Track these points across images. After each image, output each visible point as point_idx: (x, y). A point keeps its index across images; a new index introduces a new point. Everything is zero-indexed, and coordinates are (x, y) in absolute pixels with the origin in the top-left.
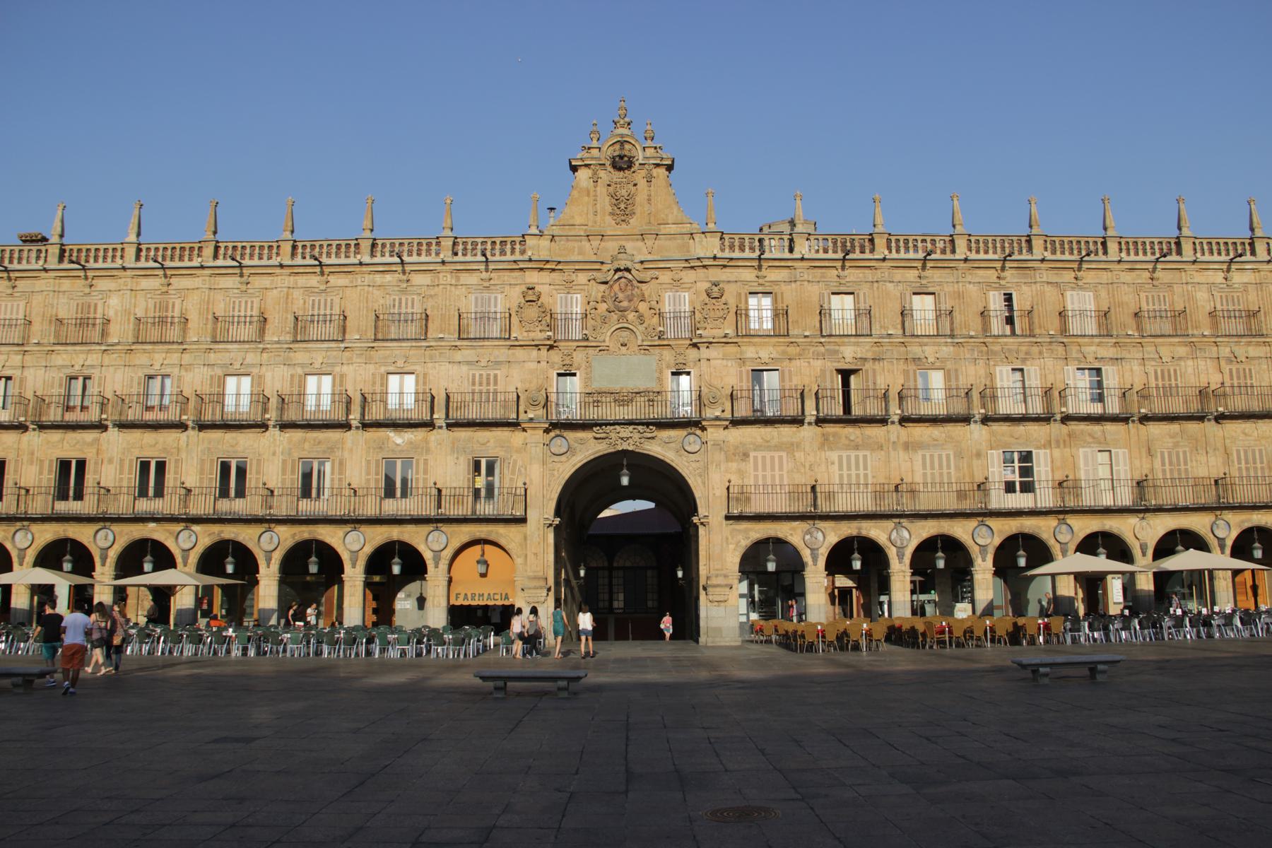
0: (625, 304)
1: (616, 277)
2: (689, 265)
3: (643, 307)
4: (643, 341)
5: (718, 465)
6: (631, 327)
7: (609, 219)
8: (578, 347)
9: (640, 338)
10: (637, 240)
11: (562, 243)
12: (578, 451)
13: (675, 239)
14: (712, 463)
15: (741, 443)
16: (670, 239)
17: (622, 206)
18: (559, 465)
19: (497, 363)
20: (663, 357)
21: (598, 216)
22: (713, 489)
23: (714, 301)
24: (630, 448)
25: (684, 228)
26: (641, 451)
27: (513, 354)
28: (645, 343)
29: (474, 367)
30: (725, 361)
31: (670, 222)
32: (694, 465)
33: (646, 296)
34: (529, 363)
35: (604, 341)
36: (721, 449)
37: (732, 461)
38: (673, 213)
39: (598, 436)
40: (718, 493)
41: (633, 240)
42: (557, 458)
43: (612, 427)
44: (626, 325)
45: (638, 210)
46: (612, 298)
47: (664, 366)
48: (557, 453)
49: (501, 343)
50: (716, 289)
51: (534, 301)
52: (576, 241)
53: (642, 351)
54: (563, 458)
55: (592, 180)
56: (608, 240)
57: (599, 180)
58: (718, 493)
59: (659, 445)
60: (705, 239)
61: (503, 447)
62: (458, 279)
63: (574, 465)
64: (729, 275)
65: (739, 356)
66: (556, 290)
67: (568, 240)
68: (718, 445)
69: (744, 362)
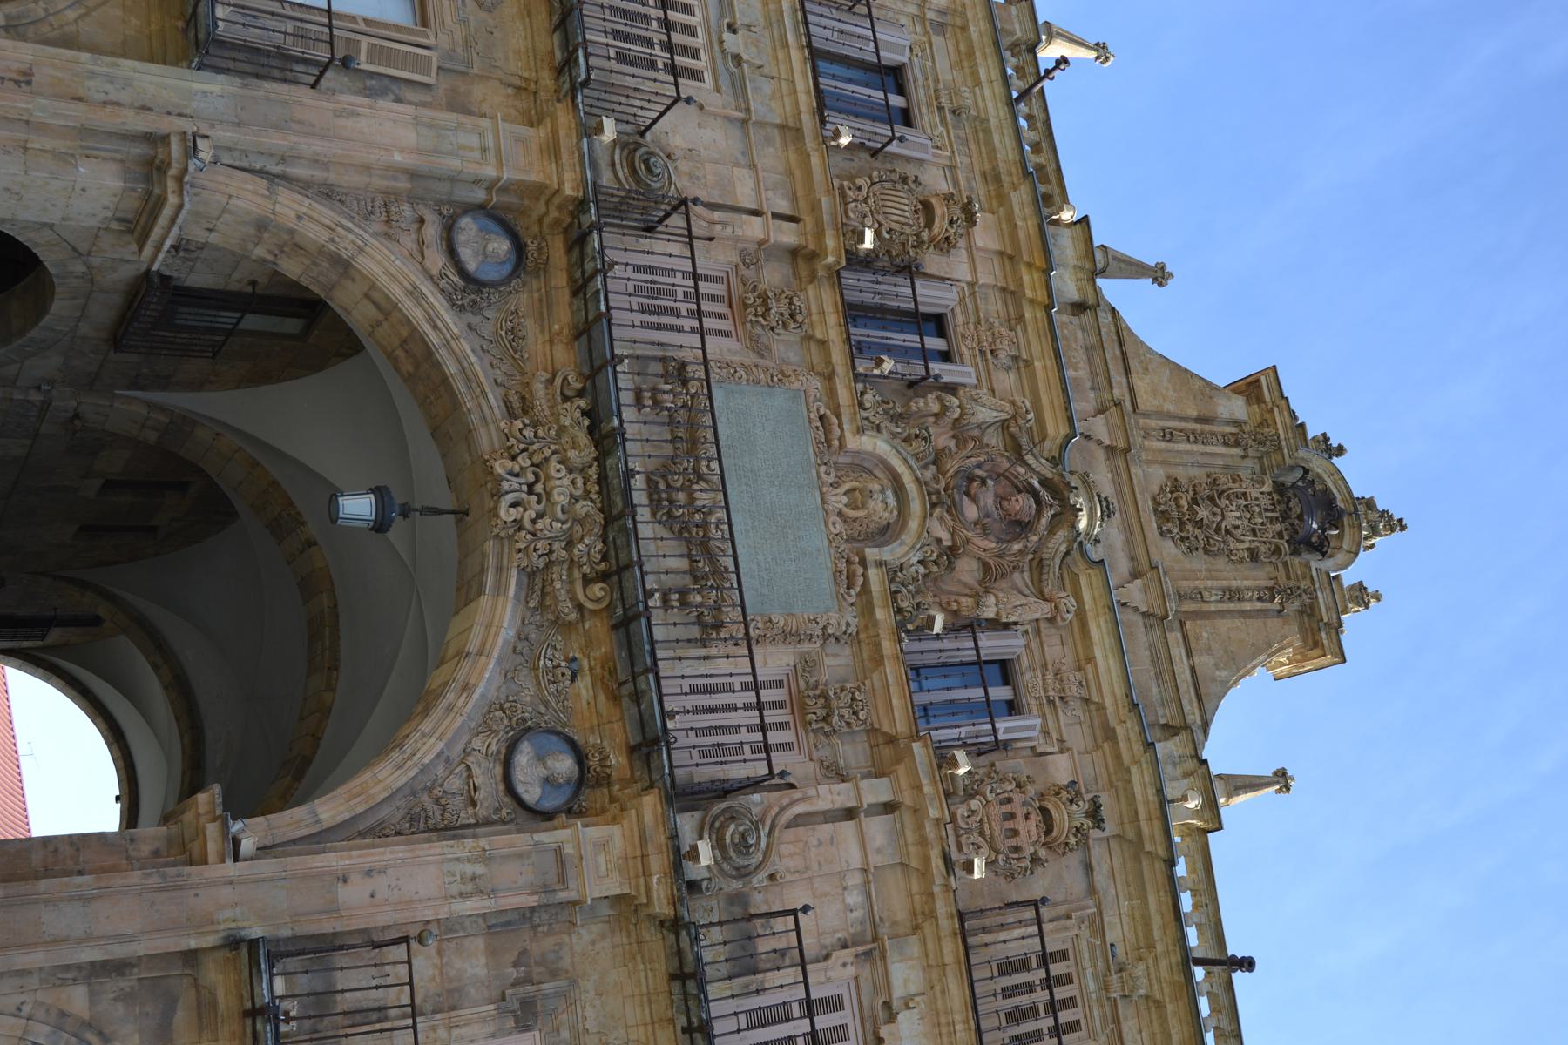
0: (971, 511)
1: (1036, 484)
2: (1113, 722)
3: (967, 570)
4: (880, 564)
5: (476, 886)
6: (913, 525)
7: (1158, 475)
8: (823, 343)
9: (892, 553)
10: (1133, 559)
11: (1080, 334)
12: (470, 317)
13: (1159, 675)
14: (485, 858)
15: (573, 983)
16: (1155, 661)
17: (1203, 513)
18: (409, 241)
19: (739, 87)
20: (832, 646)
21: (1162, 445)
22: (369, 873)
23: (1036, 818)
24: (506, 514)
25: (1190, 702)
26: (491, 562)
27: (769, 141)
28: (873, 573)
29: (713, 12)
30: (855, 879)
31: (1196, 659)
32: (455, 783)
33: (1002, 584)
34: (750, 183)
35: (860, 431)
36: (546, 889)
37: (492, 952)
38: (1217, 666)
39: (539, 389)
40: (352, 894)
41: (1129, 541)
42: (432, 231)
43: (583, 438)
44: (916, 507)
45: (1199, 562)
46: (979, 466)
47: (806, 647)
48: (461, 238)
49: (802, 98)
50: (1079, 816)
51: (929, 224)
52: (1093, 375)
53: (843, 566)
54: (437, 260)
55: (1234, 430)
56: (1114, 471)
57: (1238, 451)
58: (352, 894)
59: (522, 637)
60: (1179, 771)
61: (467, 45)
62: (941, 28)
63: (415, 293)
64: (1106, 867)
65: (884, 931)
66: (962, 301)
67: (1089, 350)
68: (563, 879)
69: (868, 954)
